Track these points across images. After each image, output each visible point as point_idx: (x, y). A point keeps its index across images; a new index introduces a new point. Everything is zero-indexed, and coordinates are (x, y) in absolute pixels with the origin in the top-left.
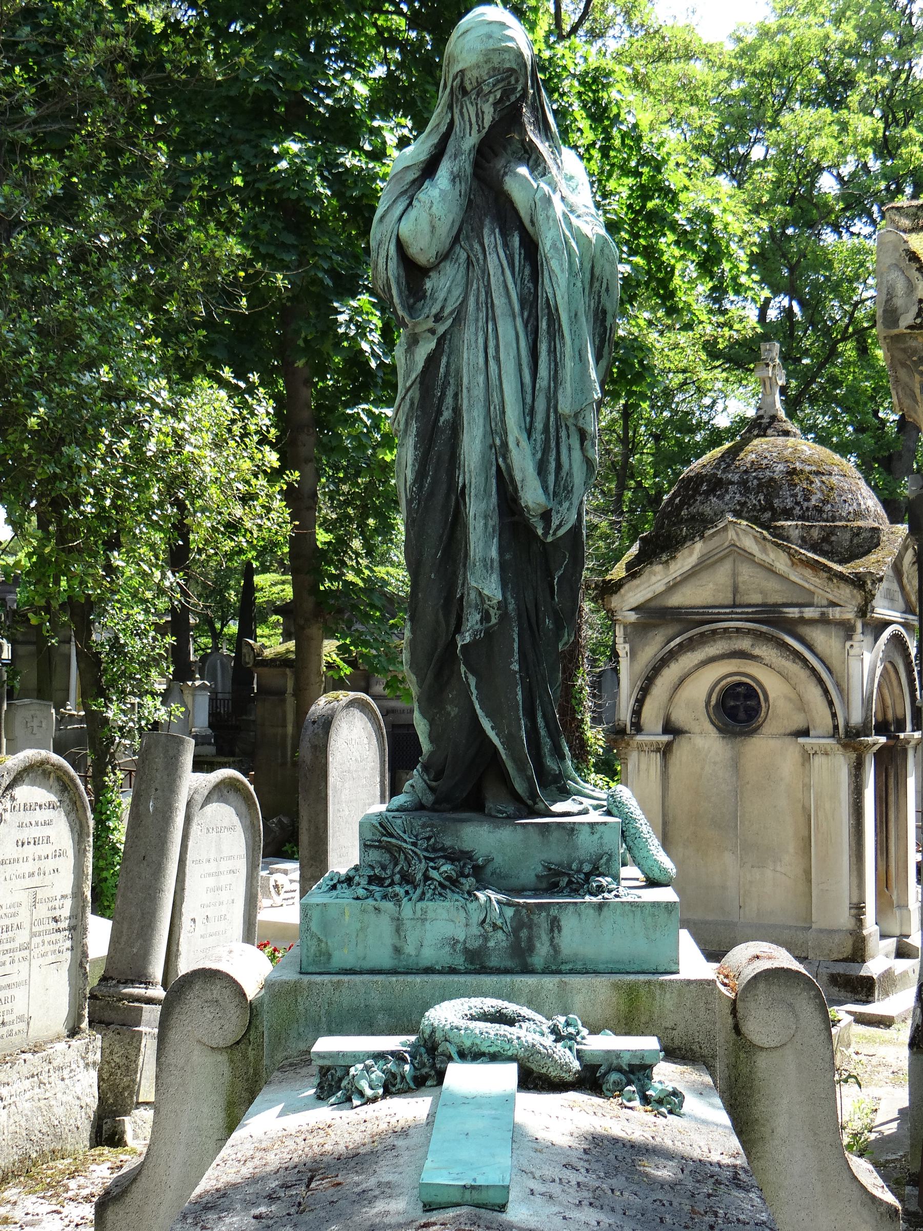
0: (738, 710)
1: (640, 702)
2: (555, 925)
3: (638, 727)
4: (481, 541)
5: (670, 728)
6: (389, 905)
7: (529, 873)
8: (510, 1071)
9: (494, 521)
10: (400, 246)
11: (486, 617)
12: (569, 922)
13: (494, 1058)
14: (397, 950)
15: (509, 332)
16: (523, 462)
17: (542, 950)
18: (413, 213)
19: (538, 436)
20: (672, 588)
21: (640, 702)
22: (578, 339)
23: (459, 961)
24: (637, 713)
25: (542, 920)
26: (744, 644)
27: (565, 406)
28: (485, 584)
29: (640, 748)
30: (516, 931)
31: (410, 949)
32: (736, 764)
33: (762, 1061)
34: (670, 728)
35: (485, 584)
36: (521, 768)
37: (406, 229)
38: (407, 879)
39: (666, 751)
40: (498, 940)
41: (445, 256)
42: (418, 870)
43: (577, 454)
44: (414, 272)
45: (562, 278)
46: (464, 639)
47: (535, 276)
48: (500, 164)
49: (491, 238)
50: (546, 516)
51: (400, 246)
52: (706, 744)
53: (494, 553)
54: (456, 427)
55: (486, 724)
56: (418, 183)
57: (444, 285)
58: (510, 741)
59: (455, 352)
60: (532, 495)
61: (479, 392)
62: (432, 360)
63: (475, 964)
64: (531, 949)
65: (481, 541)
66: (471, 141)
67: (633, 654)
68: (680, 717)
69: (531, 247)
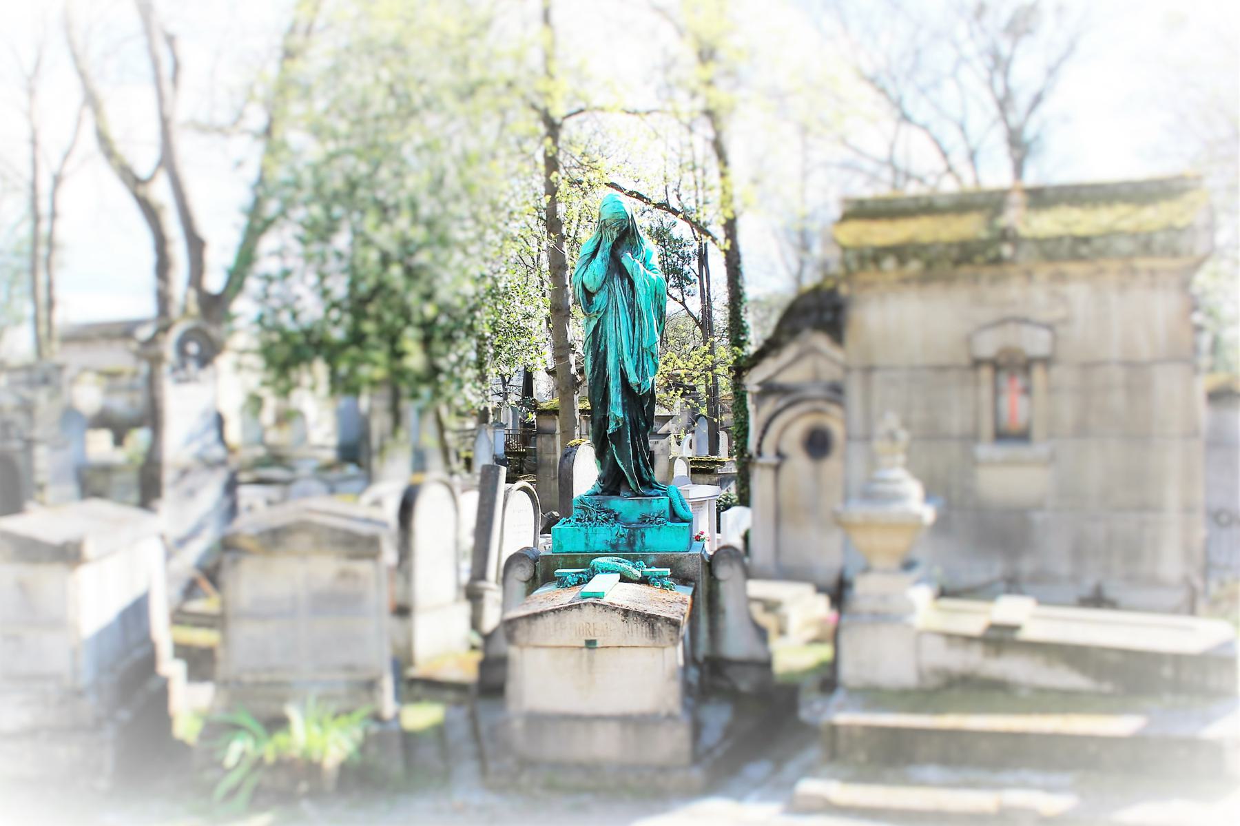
0: (818, 444)
1: (761, 439)
2: (643, 535)
3: (759, 453)
4: (615, 396)
5: (780, 455)
6: (583, 529)
7: (634, 518)
8: (618, 576)
9: (620, 388)
10: (583, 285)
11: (618, 423)
12: (648, 533)
13: (613, 572)
14: (587, 545)
15: (624, 318)
16: (630, 367)
17: (639, 543)
18: (587, 274)
19: (635, 356)
20: (780, 371)
21: (761, 439)
22: (650, 319)
23: (609, 549)
24: (759, 445)
25: (638, 533)
26: (820, 405)
27: (645, 345)
28: (616, 410)
29: (762, 466)
30: (629, 536)
31: (591, 544)
32: (817, 477)
33: (722, 586)
34: (780, 455)
35: (616, 410)
36: (633, 478)
37: (585, 279)
38: (590, 519)
39: (777, 468)
40: (623, 541)
41: (600, 288)
42: (594, 516)
43: (651, 362)
44: (589, 295)
45: (643, 298)
46: (609, 432)
47: (634, 296)
48: (620, 251)
49: (617, 281)
50: (639, 386)
51: (583, 285)
52: (799, 463)
53: (620, 400)
54: (605, 352)
55: (620, 463)
56: (589, 261)
57: (599, 300)
58: (629, 469)
59: (604, 324)
60: (633, 379)
61: (613, 340)
62: (596, 328)
63: (614, 549)
64: (634, 544)
65: (615, 396)
66: (609, 244)
67: (757, 410)
68: (786, 447)
69: (632, 283)
